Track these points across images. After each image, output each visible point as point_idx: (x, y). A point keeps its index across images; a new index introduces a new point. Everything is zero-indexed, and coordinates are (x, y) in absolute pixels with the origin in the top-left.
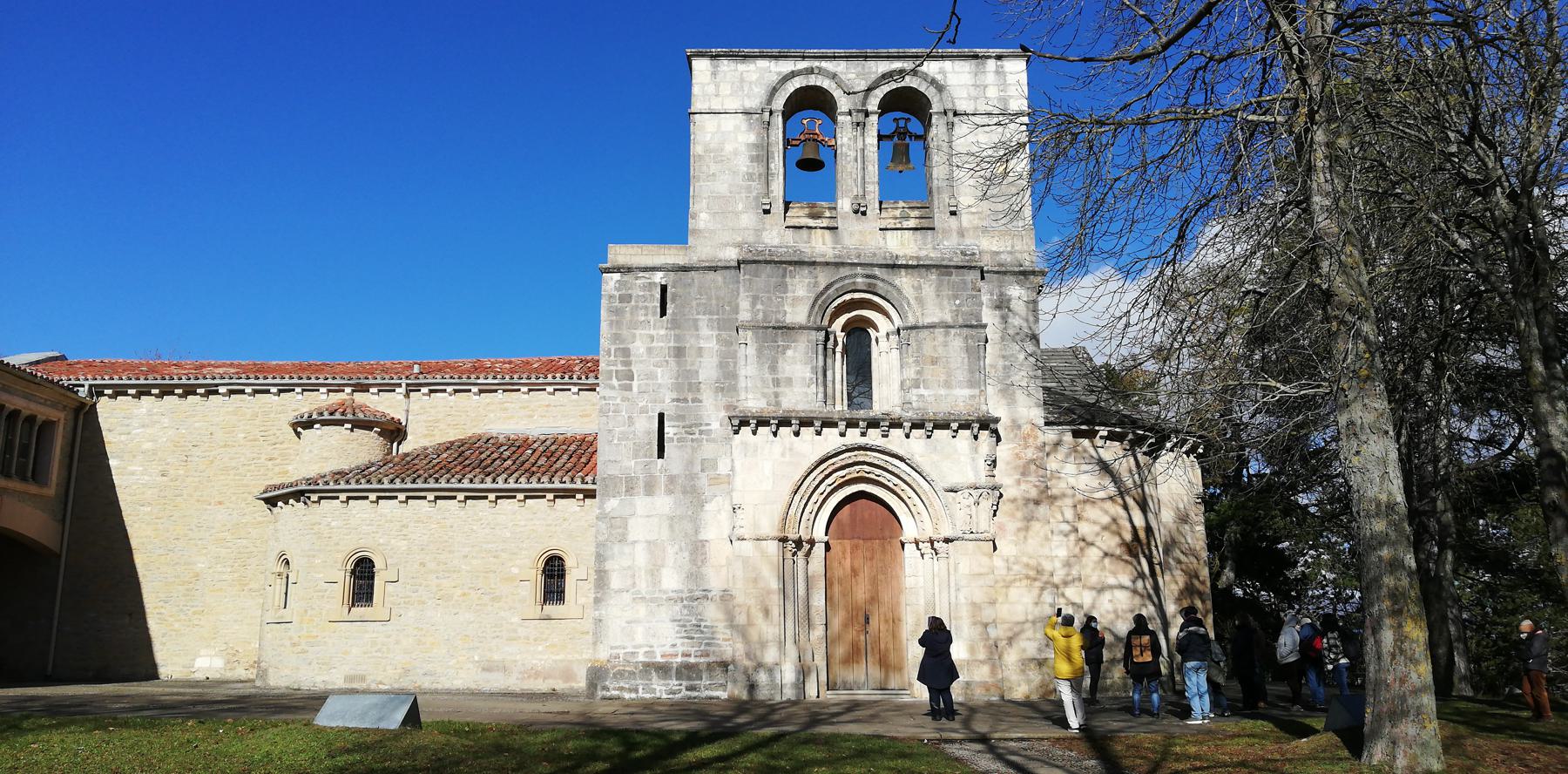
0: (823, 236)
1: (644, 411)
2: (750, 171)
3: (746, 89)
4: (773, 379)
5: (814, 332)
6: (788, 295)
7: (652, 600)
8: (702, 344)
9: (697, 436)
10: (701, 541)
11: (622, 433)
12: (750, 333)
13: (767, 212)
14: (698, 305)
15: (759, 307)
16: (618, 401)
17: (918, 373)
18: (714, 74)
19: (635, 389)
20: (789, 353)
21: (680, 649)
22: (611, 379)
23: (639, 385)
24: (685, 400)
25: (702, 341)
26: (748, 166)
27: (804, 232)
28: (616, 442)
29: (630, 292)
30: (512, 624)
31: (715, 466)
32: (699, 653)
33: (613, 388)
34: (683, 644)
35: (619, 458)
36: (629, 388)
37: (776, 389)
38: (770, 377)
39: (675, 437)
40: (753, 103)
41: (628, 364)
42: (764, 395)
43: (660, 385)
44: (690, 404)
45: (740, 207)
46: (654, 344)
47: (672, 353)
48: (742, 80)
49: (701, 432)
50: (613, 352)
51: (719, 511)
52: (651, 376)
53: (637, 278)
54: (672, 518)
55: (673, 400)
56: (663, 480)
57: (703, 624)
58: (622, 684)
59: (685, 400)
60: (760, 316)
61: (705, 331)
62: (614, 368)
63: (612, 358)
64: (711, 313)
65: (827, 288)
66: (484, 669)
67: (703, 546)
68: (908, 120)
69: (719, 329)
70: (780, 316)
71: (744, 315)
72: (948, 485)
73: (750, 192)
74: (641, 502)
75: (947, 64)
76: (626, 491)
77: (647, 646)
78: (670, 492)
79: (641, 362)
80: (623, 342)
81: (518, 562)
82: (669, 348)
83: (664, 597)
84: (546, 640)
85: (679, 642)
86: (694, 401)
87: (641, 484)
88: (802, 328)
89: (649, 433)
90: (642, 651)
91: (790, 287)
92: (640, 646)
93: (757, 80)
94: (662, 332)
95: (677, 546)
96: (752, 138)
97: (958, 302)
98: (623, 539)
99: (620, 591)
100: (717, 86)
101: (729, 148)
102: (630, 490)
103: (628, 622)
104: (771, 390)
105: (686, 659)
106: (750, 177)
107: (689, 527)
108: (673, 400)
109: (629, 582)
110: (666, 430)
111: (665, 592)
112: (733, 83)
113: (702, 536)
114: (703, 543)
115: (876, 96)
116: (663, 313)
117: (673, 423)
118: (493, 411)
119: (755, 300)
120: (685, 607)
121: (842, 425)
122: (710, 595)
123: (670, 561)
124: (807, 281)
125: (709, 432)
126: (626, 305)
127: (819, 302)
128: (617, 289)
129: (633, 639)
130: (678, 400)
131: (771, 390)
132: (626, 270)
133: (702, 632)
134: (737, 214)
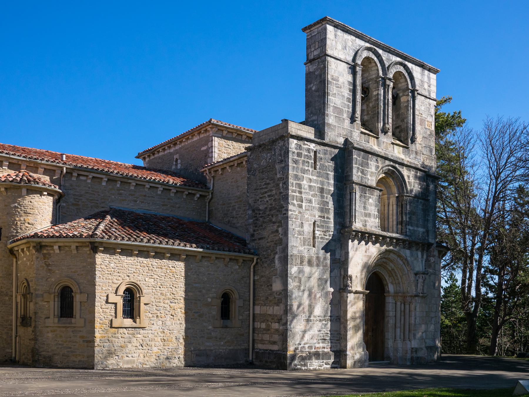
19: (304, 208)
22: (293, 200)
24: (324, 217)
25: (330, 186)
28: (296, 236)
30: (209, 330)
33: (294, 205)
36: (300, 206)
38: (364, 211)
46: (312, 184)
50: (294, 184)
51: (336, 277)
52: (310, 201)
53: (304, 144)
55: (319, 216)
59: (324, 217)
66: (197, 355)
75: (414, 66)
76: (301, 263)
79: (306, 193)
81: (211, 295)
82: (318, 187)
94: (315, 178)
110: (316, 232)
115: (391, 72)
117: (319, 229)
119: (358, 168)
126: (300, 159)
128: (296, 149)
132: (300, 138)
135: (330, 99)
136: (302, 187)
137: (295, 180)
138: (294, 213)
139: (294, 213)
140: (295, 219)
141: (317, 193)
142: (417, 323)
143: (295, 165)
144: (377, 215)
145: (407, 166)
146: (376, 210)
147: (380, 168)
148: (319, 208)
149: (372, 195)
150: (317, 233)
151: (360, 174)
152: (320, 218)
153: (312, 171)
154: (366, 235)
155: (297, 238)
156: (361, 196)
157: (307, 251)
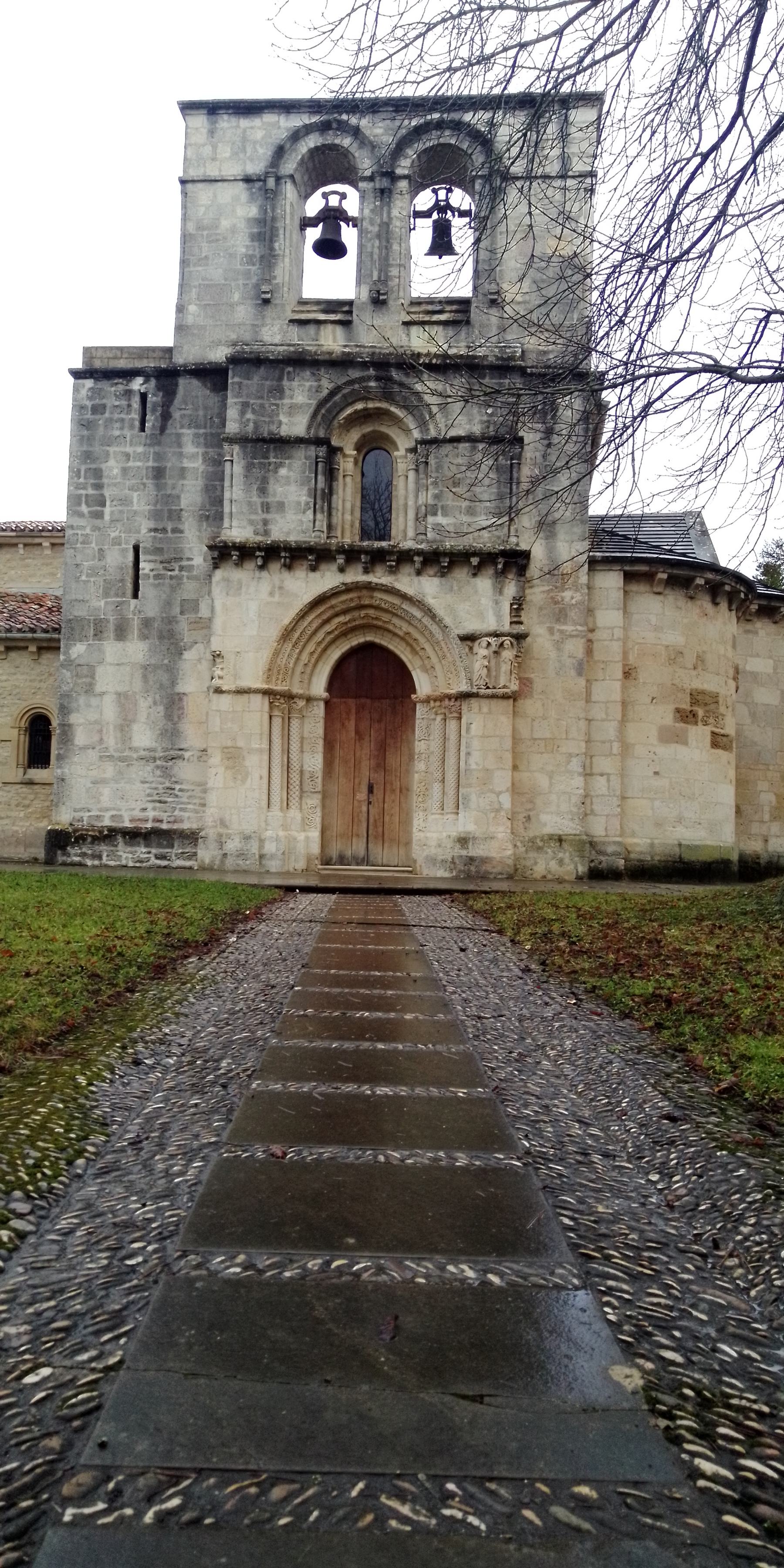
0: (334, 333)
1: (117, 542)
2: (250, 252)
3: (249, 150)
4: (262, 504)
5: (313, 448)
6: (286, 401)
7: (122, 759)
8: (186, 464)
9: (176, 572)
10: (178, 694)
11: (91, 568)
12: (236, 448)
13: (266, 302)
14: (183, 416)
15: (249, 415)
16: (88, 531)
17: (437, 497)
18: (212, 132)
19: (107, 517)
20: (283, 471)
21: (151, 814)
22: (79, 504)
23: (112, 513)
24: (164, 530)
26: (247, 247)
27: (311, 329)
28: (84, 578)
29: (104, 401)
31: (196, 608)
32: (172, 819)
34: (154, 809)
35: (87, 597)
36: (99, 515)
37: (265, 516)
39: (152, 574)
40: (255, 168)
41: (98, 486)
42: (251, 522)
43: (135, 512)
44: (170, 535)
45: (236, 297)
46: (131, 464)
47: (150, 475)
48: (244, 139)
49: (182, 568)
50: (82, 473)
52: (125, 501)
54: (145, 668)
55: (151, 530)
56: (136, 623)
57: (178, 787)
58: (84, 850)
60: (250, 427)
61: (190, 448)
62: (83, 492)
63: (82, 480)
64: (197, 427)
65: (332, 394)
67: (181, 700)
68: (449, 191)
69: (206, 445)
70: (273, 428)
71: (232, 427)
72: (462, 632)
73: (249, 278)
74: (111, 648)
76: (95, 635)
77: (114, 809)
78: (144, 637)
79: (115, 485)
80: (94, 461)
82: (147, 468)
83: (135, 756)
84: (28, 806)
85: (150, 806)
86: (175, 530)
87: (111, 627)
88: (299, 441)
89: (122, 569)
90: (108, 815)
91: (287, 392)
92: (107, 810)
93: (263, 138)
94: (140, 449)
95: (150, 699)
96: (253, 211)
97: (489, 411)
98: (89, 690)
99: (85, 748)
100: (214, 147)
101: (225, 224)
102: (99, 634)
103: (94, 783)
104: (259, 516)
105: (157, 825)
106: (250, 260)
107: (164, 678)
108: (151, 530)
109: (96, 738)
110: (142, 565)
111: (136, 750)
112: (233, 144)
113: (180, 688)
114: (181, 696)
116: (142, 428)
118: (12, 568)
119: (245, 406)
120: (158, 767)
121: (341, 560)
122: (187, 755)
123: (142, 716)
124: (308, 384)
125: (190, 568)
126: (97, 417)
127: (323, 411)
128: (90, 398)
129: (99, 802)
130: (156, 530)
131: (259, 516)
133: (177, 796)
134: (232, 306)
135: (190, 272)
136: (105, 474)
137: (86, 463)
138: (79, 532)
139: (79, 532)
140: (83, 543)
141: (145, 480)
142: (473, 766)
143: (85, 433)
144: (307, 503)
145: (430, 367)
146: (305, 491)
147: (325, 392)
148: (149, 511)
149: (288, 458)
150: (145, 567)
151: (249, 415)
152: (152, 534)
153: (132, 436)
154: (258, 553)
155: (85, 582)
156: (249, 467)
157: (113, 607)
